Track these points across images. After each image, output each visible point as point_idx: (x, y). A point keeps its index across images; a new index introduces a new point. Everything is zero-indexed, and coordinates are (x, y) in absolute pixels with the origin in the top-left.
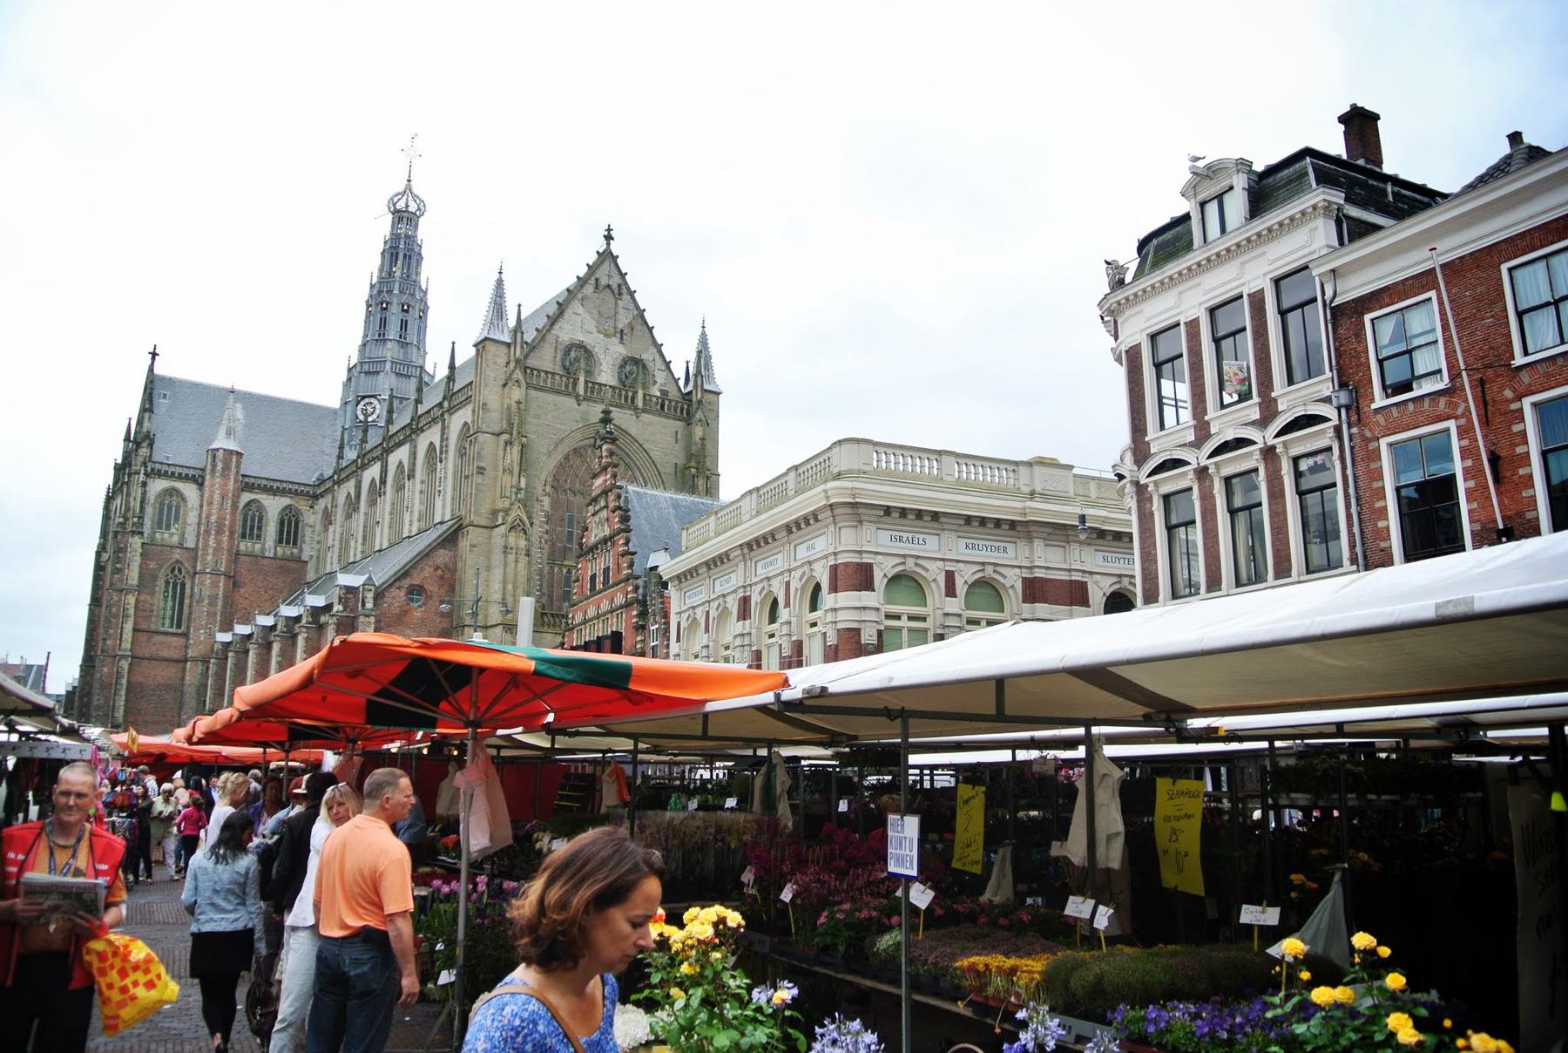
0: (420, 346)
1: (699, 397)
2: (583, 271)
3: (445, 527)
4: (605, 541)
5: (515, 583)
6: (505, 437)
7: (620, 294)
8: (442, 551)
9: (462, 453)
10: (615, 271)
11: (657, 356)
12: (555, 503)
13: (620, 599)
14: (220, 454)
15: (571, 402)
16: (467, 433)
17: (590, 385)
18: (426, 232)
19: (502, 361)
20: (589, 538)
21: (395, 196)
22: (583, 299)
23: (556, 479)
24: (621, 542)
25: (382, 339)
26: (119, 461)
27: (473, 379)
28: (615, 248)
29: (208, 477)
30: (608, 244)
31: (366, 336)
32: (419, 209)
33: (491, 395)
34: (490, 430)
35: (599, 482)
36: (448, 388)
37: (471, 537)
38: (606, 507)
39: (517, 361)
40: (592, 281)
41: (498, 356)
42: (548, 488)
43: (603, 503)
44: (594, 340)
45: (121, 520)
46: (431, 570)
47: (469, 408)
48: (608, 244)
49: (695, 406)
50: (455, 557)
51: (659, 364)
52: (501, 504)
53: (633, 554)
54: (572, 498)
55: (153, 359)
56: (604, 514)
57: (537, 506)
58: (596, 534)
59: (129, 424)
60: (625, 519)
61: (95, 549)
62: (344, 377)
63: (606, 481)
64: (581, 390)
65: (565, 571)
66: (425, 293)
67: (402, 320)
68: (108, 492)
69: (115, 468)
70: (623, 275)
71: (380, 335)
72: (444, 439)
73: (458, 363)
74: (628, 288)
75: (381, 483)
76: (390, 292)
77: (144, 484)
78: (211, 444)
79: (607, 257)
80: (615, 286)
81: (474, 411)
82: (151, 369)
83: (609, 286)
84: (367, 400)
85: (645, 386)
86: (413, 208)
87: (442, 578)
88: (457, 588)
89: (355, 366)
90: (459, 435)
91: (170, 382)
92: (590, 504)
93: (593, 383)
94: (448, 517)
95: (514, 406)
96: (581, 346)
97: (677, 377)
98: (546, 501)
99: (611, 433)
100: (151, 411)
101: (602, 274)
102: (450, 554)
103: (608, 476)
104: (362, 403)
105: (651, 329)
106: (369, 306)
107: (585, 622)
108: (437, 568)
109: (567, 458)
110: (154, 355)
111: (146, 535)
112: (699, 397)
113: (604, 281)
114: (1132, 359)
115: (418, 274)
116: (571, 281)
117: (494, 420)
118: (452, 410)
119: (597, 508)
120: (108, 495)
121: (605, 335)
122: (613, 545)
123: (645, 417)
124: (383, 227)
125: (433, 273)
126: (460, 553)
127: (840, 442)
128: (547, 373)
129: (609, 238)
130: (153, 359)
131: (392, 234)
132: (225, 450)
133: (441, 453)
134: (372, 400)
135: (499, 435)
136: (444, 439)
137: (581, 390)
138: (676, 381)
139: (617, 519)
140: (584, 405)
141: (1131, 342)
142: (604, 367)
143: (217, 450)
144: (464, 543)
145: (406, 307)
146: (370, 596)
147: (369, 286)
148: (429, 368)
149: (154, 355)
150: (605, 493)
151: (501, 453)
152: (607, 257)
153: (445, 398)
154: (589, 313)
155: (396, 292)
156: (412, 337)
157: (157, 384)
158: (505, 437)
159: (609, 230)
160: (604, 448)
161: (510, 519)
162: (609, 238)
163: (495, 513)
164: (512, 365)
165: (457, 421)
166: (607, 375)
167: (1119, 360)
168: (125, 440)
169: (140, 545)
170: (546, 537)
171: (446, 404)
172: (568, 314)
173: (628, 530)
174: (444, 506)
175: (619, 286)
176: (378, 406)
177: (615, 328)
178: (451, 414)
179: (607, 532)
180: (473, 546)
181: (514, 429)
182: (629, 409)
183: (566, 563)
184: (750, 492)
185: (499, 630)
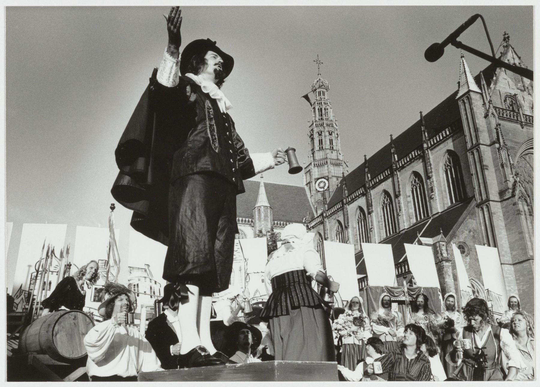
10: (515, 56)
29: (257, 221)
46: (467, 232)
67: (330, 140)
71: (320, 148)
75: (368, 207)
93: (526, 115)
108: (470, 232)
121: (521, 90)
134: (323, 180)
142: (525, 108)
145: (330, 133)
146: (444, 248)
158: (497, 145)
177: (524, 86)
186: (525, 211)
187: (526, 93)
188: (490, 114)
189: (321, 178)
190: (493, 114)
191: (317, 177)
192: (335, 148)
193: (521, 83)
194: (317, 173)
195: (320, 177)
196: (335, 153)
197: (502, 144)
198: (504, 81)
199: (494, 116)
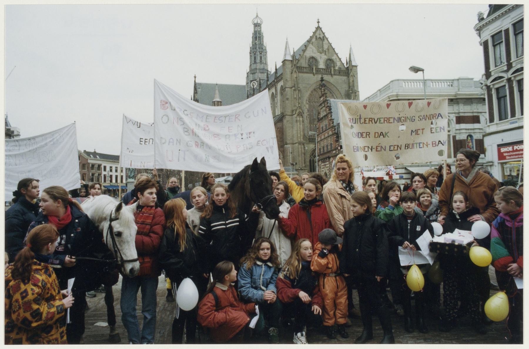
0: (266, 64)
1: (351, 68)
2: (311, 34)
3: (278, 117)
4: (325, 116)
5: (300, 131)
6: (293, 88)
7: (324, 39)
8: (279, 123)
9: (282, 94)
11: (337, 57)
12: (310, 106)
13: (330, 133)
14: (216, 102)
15: (312, 75)
16: (283, 89)
17: (317, 69)
18: (265, 30)
19: (290, 66)
20: (320, 116)
21: (254, 19)
22: (312, 43)
23: (309, 99)
24: (330, 116)
25: (255, 62)
27: (282, 72)
28: (321, 26)
30: (318, 24)
31: (251, 63)
32: (261, 22)
33: (288, 75)
34: (289, 87)
35: (322, 99)
36: (276, 76)
37: (288, 118)
38: (324, 106)
39: (295, 65)
40: (315, 37)
41: (289, 65)
42: (307, 102)
43: (323, 105)
44: (317, 55)
47: (282, 81)
48: (318, 24)
49: (350, 71)
50: (283, 124)
51: (338, 60)
52: (294, 108)
53: (333, 119)
54: (314, 104)
55: (195, 78)
56: (324, 108)
57: (305, 107)
58: (322, 114)
60: (330, 109)
62: (246, 75)
63: (324, 99)
64: (314, 71)
65: (314, 125)
66: (266, 47)
70: (324, 33)
72: (276, 91)
73: (277, 68)
74: (326, 37)
76: (256, 48)
78: (213, 99)
79: (318, 28)
80: (322, 37)
81: (284, 82)
82: (195, 81)
83: (320, 38)
84: (253, 82)
85: (334, 67)
86: (259, 22)
87: (280, 131)
88: (284, 133)
89: (249, 72)
90: (281, 89)
91: (200, 84)
92: (319, 106)
93: (318, 69)
94: (279, 114)
95: (295, 79)
96: (313, 58)
97: (343, 63)
98: (307, 106)
99: (324, 84)
100: (196, 93)
101: (317, 34)
102: (281, 124)
103: (324, 97)
104: (252, 83)
105: (334, 49)
106: (250, 53)
107: (321, 140)
109: (312, 92)
110: (195, 77)
112: (351, 68)
113: (318, 36)
114: (485, 45)
115: (263, 42)
116: (308, 38)
117: (289, 84)
118: (278, 82)
119: (322, 107)
122: (328, 117)
123: (335, 77)
124: (251, 29)
125: (267, 41)
126: (284, 124)
127: (392, 81)
128: (304, 67)
129: (318, 22)
130: (195, 78)
131: (254, 31)
132: (217, 101)
133: (276, 95)
134: (255, 81)
135: (291, 88)
136: (276, 91)
137: (314, 71)
138: (343, 64)
139: (328, 110)
140: (316, 76)
141: (485, 39)
143: (215, 101)
144: (285, 121)
147: (250, 48)
148: (269, 70)
149: (195, 77)
150: (324, 102)
151: (293, 94)
152: (318, 28)
153: (275, 79)
154: (315, 47)
155: (257, 48)
156: (264, 61)
157: (197, 85)
158: (293, 88)
159: (318, 20)
160: (322, 89)
161: (297, 112)
162: (318, 22)
163: (293, 111)
164: (293, 67)
165: (279, 85)
166: (322, 66)
167: (481, 45)
170: (308, 116)
171: (276, 81)
172: (308, 48)
173: (331, 113)
174: (278, 111)
175: (323, 37)
176: (256, 83)
177: (323, 50)
178: (277, 84)
179: (325, 114)
180: (287, 121)
181: (295, 87)
182: (329, 75)
183: (315, 123)
184: (367, 99)
185: (297, 145)
186: (300, 121)
187: (323, 54)
188: (293, 72)
189: (254, 80)
190: (295, 71)
191: (251, 79)
192: (263, 62)
193: (322, 48)
194: (251, 78)
195: (253, 80)
196: (262, 65)
197: (296, 88)
198: (311, 49)
199: (296, 72)
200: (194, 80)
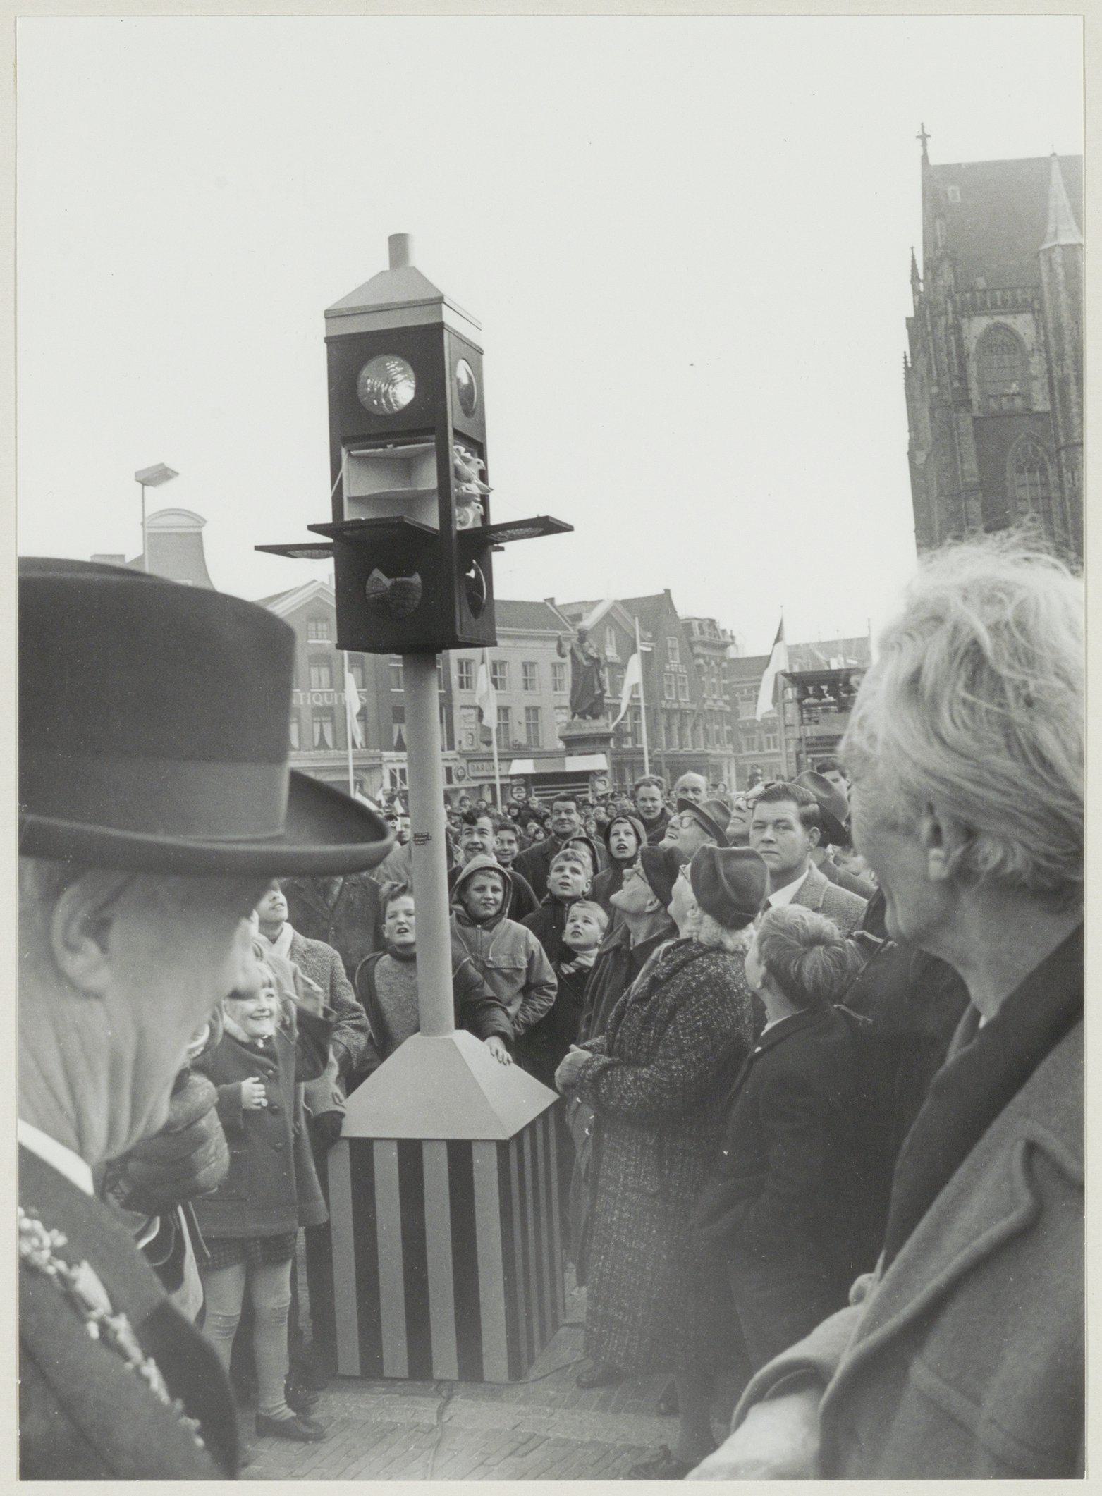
26: (911, 314)
45: (935, 390)
55: (924, 145)
59: (913, 256)
61: (906, 449)
68: (906, 363)
69: (908, 326)
77: (958, 328)
78: (1043, 241)
82: (925, 158)
110: (924, 137)
111: (975, 408)
120: (906, 368)
130: (924, 145)
132: (1063, 247)
143: (1052, 249)
149: (924, 137)
168: (912, 282)
169: (969, 420)
200: (921, 153)
